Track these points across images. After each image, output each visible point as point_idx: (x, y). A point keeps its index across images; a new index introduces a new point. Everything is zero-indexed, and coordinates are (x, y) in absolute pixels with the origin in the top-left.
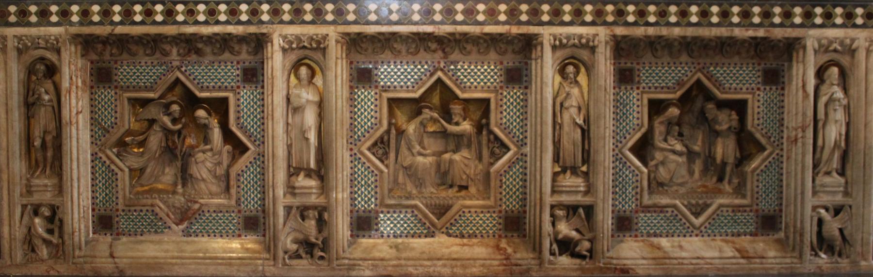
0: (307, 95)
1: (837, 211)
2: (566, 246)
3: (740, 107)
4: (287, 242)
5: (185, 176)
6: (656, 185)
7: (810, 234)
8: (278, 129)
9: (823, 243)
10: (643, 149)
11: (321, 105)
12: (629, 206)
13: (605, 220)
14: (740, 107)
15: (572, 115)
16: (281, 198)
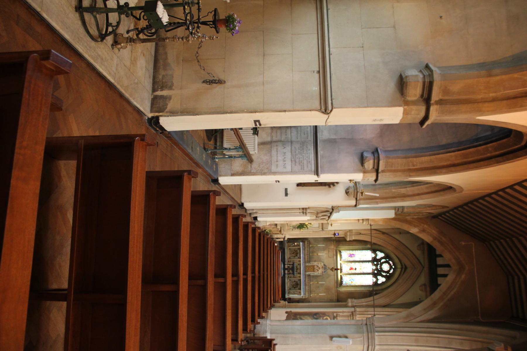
0: (297, 261)
1: (291, 293)
2: (289, 276)
3: (297, 287)
4: (289, 260)
5: (293, 254)
6: (292, 282)
7: (289, 291)
8: (295, 259)
9: (289, 292)
10: (295, 281)
11: (296, 262)
12: (291, 280)
13: (290, 279)
14: (297, 287)
15: (296, 277)
16: (291, 260)
